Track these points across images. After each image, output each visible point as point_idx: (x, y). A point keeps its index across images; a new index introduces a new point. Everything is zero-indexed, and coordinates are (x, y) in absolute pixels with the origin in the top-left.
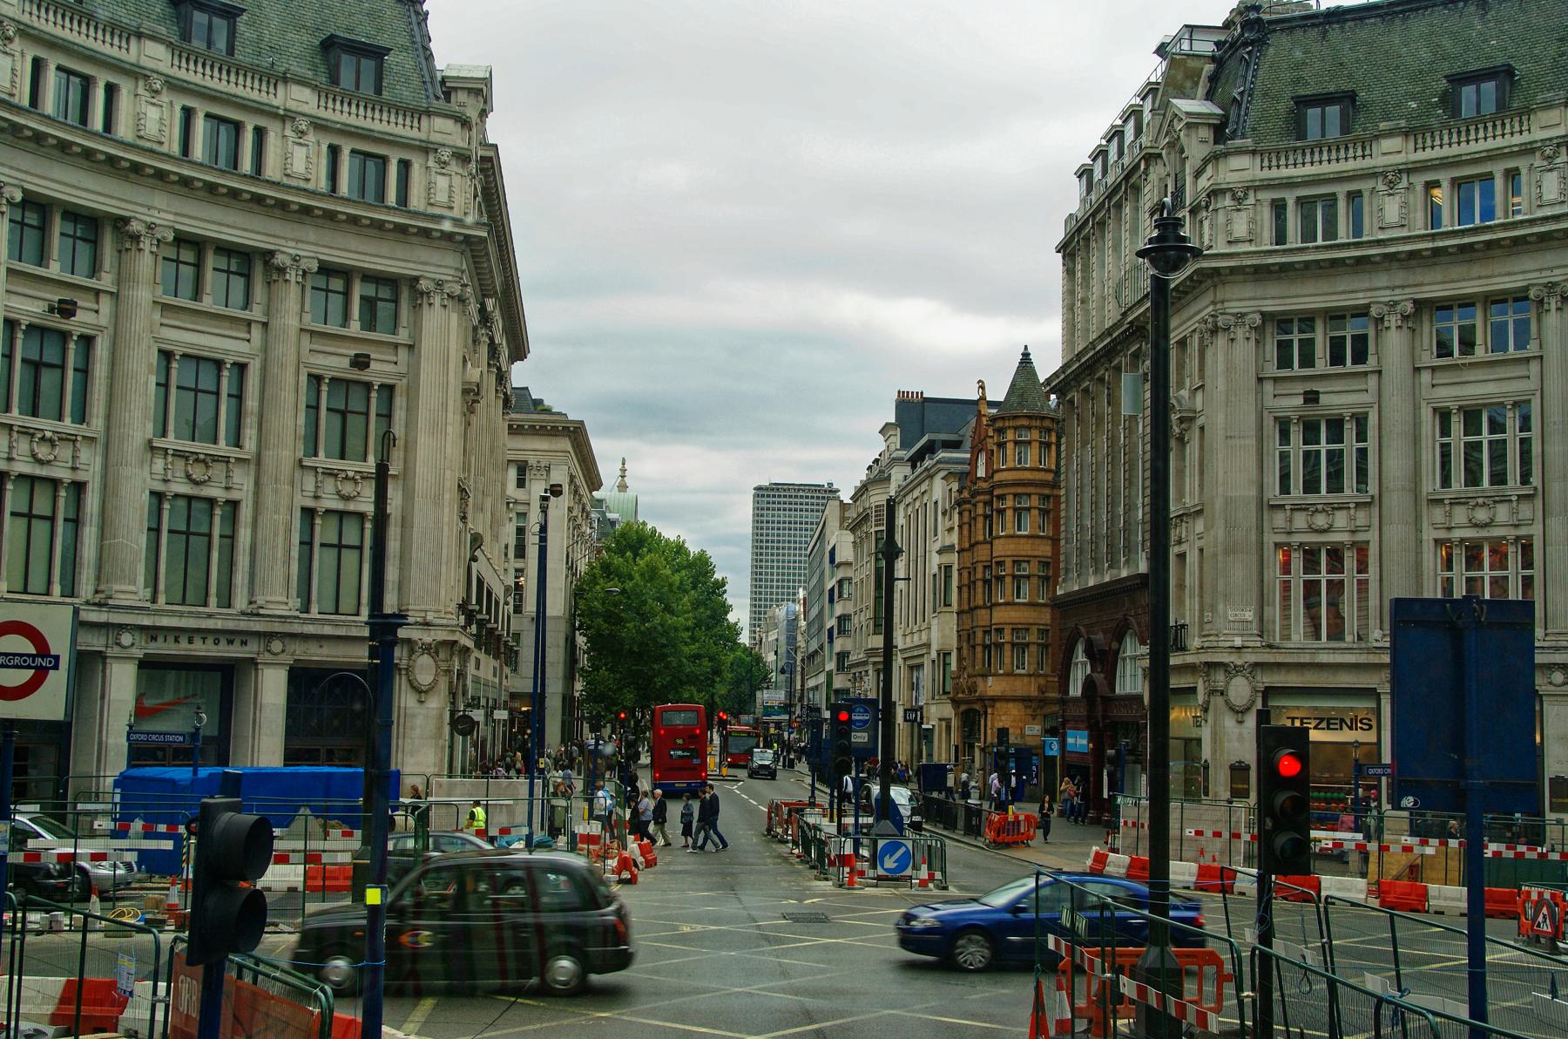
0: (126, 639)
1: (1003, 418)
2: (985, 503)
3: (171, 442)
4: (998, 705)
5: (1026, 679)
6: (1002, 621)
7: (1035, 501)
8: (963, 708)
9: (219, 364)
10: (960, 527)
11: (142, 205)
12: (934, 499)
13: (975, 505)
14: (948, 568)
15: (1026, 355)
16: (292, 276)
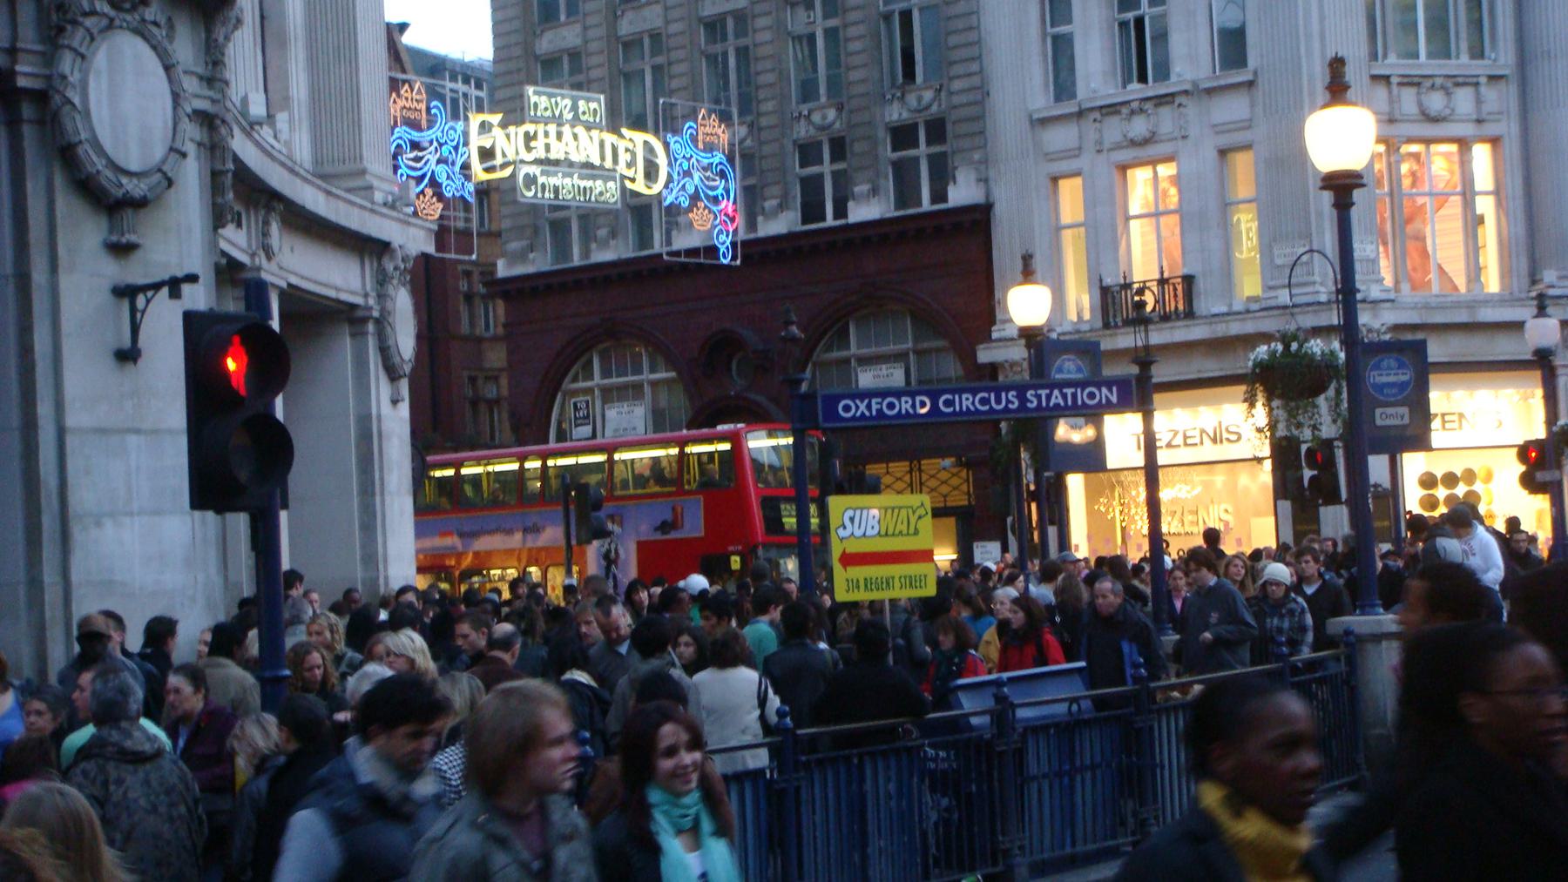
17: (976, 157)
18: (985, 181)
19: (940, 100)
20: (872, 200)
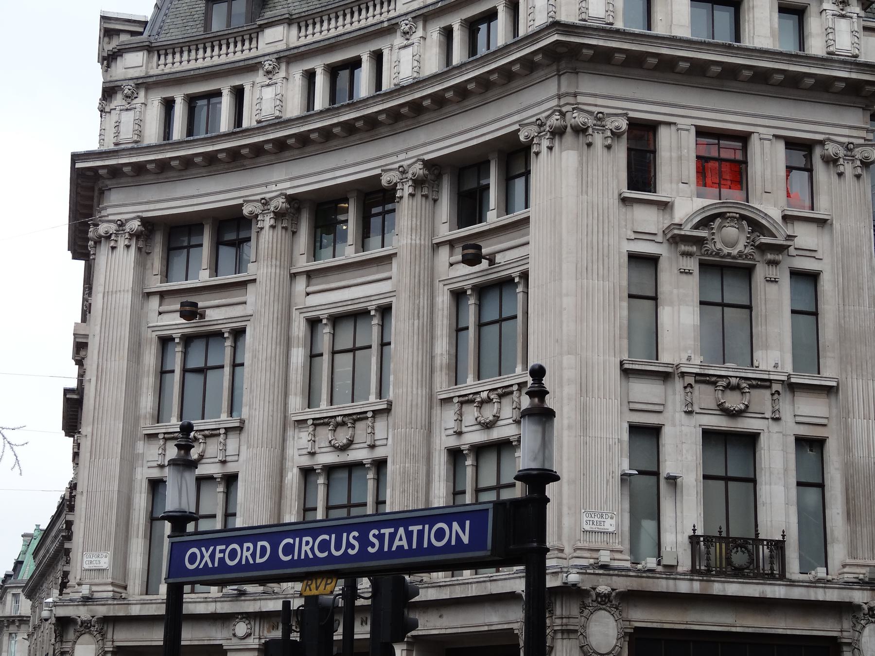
0: (241, 628)
3: (323, 408)
9: (364, 314)
11: (259, 186)
16: (406, 190)
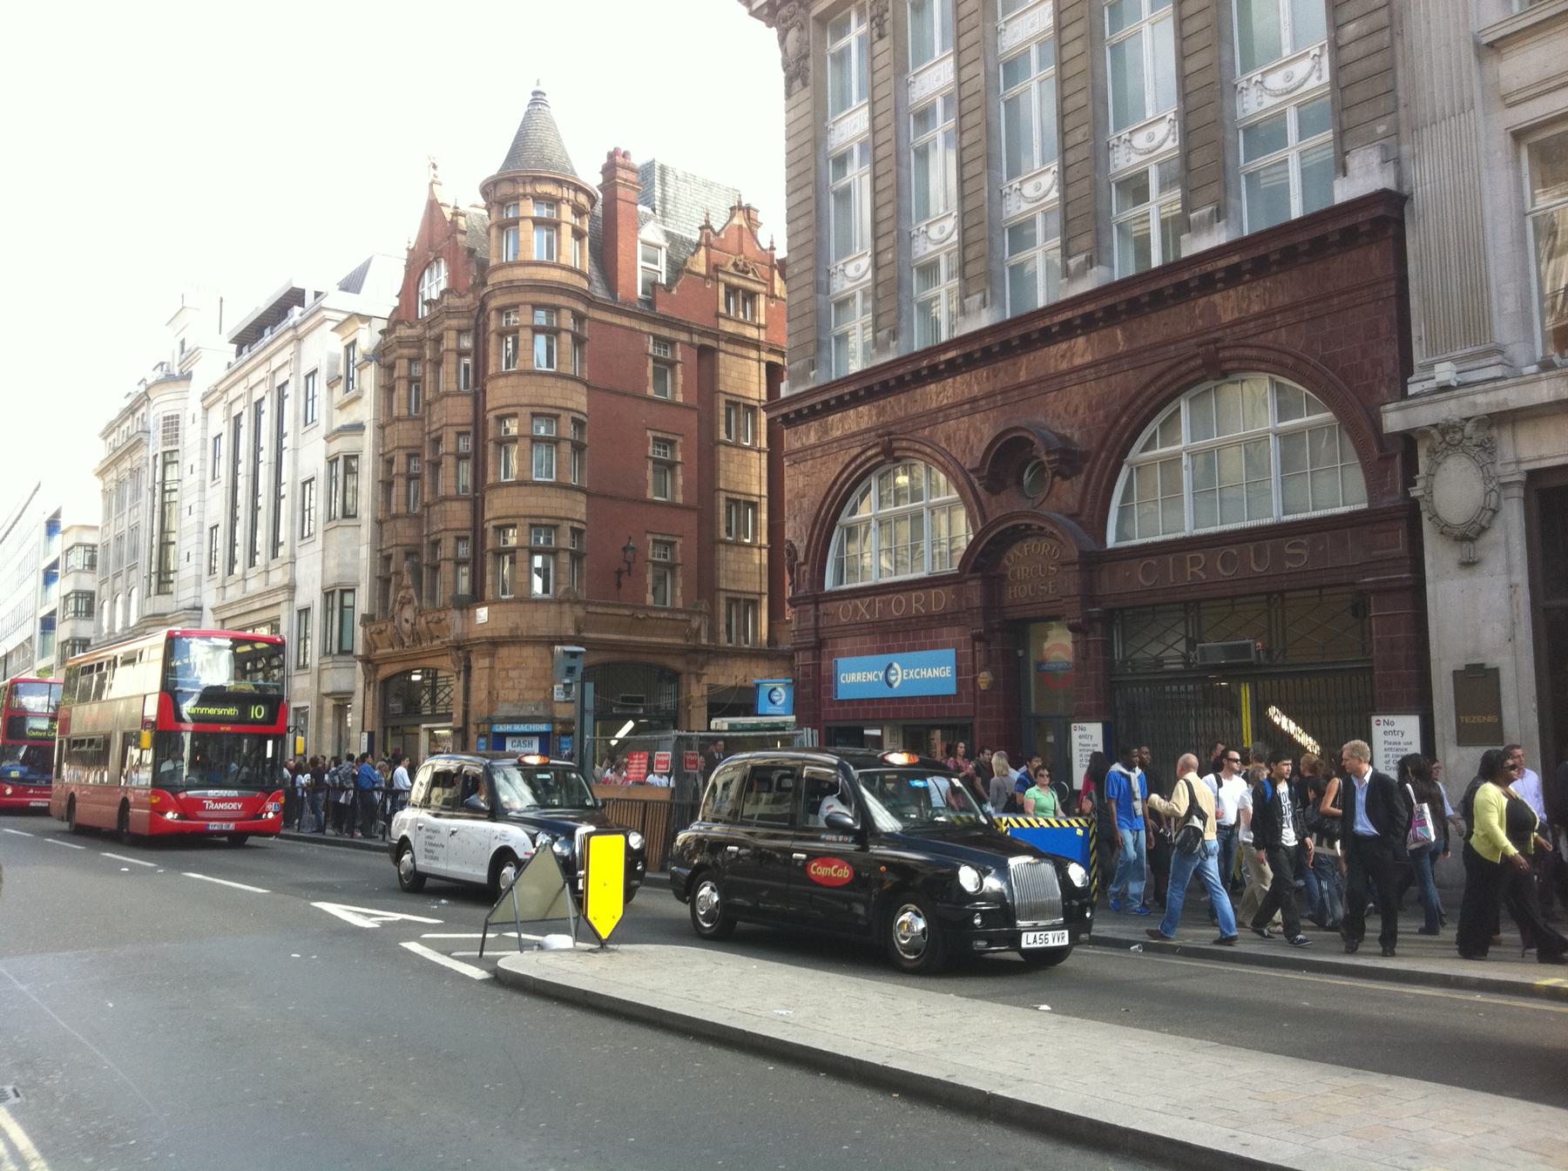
1: (513, 180)
2: (411, 360)
4: (503, 652)
5: (553, 609)
6: (512, 512)
7: (567, 321)
8: (386, 671)
10: (387, 389)
12: (306, 370)
13: (438, 340)
14: (350, 459)
15: (537, 98)
17: (1381, 129)
18: (1398, 162)
19: (1320, 70)
20: (1216, 225)
